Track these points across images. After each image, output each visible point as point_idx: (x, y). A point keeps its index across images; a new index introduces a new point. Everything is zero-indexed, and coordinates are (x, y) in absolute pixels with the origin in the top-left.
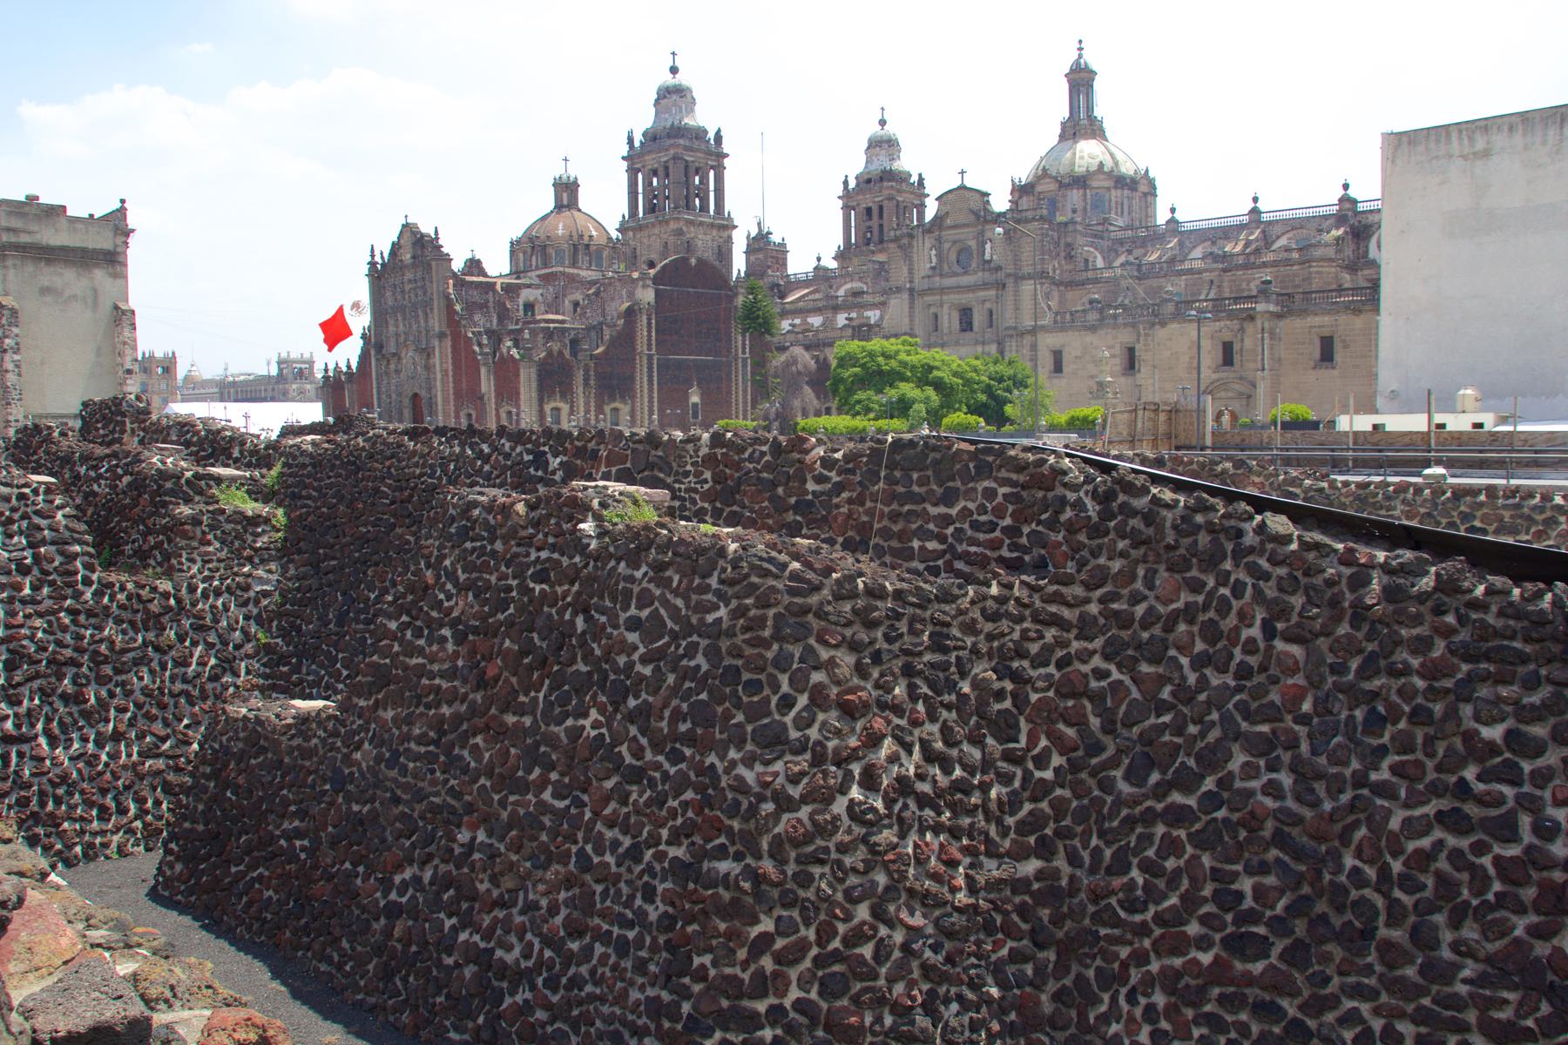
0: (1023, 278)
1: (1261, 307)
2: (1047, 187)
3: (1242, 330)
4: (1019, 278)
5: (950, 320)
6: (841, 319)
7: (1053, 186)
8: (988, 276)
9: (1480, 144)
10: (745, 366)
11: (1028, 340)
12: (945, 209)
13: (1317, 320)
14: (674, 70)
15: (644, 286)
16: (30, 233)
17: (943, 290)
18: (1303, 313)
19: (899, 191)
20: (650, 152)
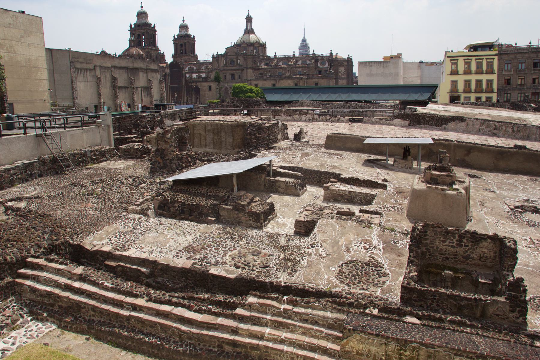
1: (304, 77)
2: (243, 45)
3: (299, 81)
4: (247, 68)
5: (229, 77)
6: (195, 76)
7: (246, 45)
8: (239, 68)
9: (371, 65)
11: (249, 82)
13: (315, 80)
14: (142, 7)
15: (168, 69)
17: (227, 70)
18: (312, 78)
20: (138, 30)
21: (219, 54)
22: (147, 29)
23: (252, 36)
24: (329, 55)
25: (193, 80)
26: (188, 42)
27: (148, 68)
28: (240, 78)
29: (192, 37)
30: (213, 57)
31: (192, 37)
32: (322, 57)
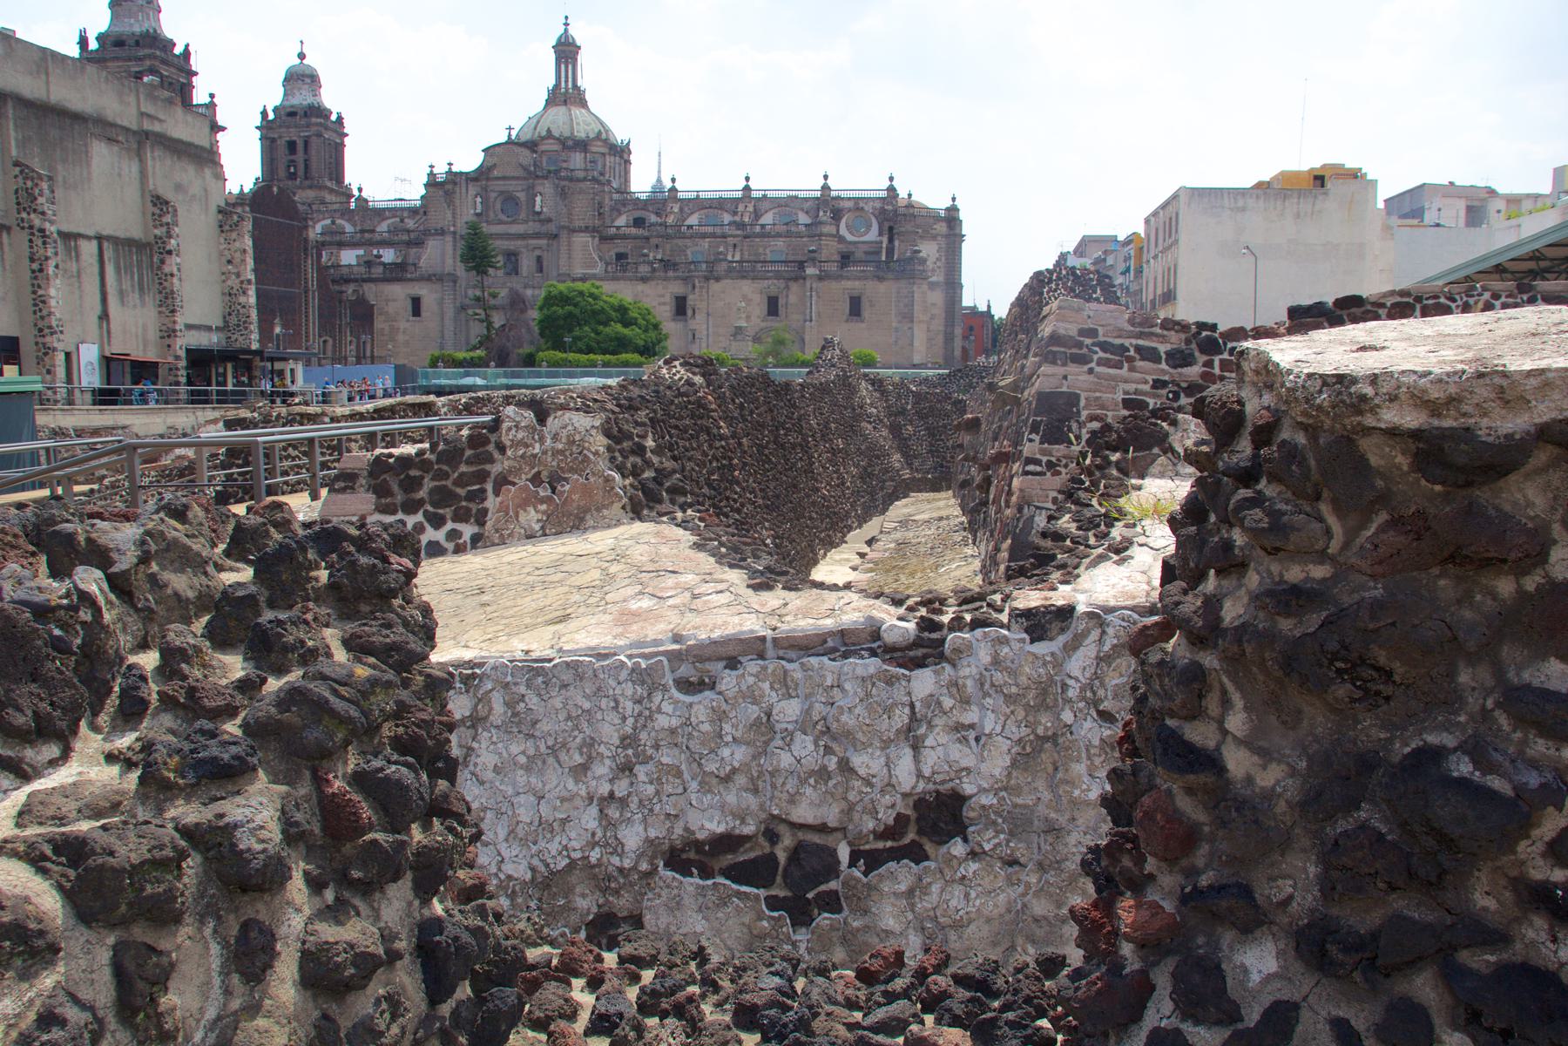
0: (573, 231)
2: (549, 146)
3: (787, 287)
6: (349, 257)
8: (537, 225)
9: (1240, 203)
10: (314, 298)
12: (491, 161)
13: (849, 284)
16: (160, 121)
19: (326, 128)
21: (454, 169)
22: (155, 57)
23: (577, 112)
24: (883, 194)
25: (345, 271)
26: (319, 135)
27: (147, 125)
28: (540, 270)
29: (334, 118)
30: (432, 183)
31: (334, 118)
32: (858, 204)
